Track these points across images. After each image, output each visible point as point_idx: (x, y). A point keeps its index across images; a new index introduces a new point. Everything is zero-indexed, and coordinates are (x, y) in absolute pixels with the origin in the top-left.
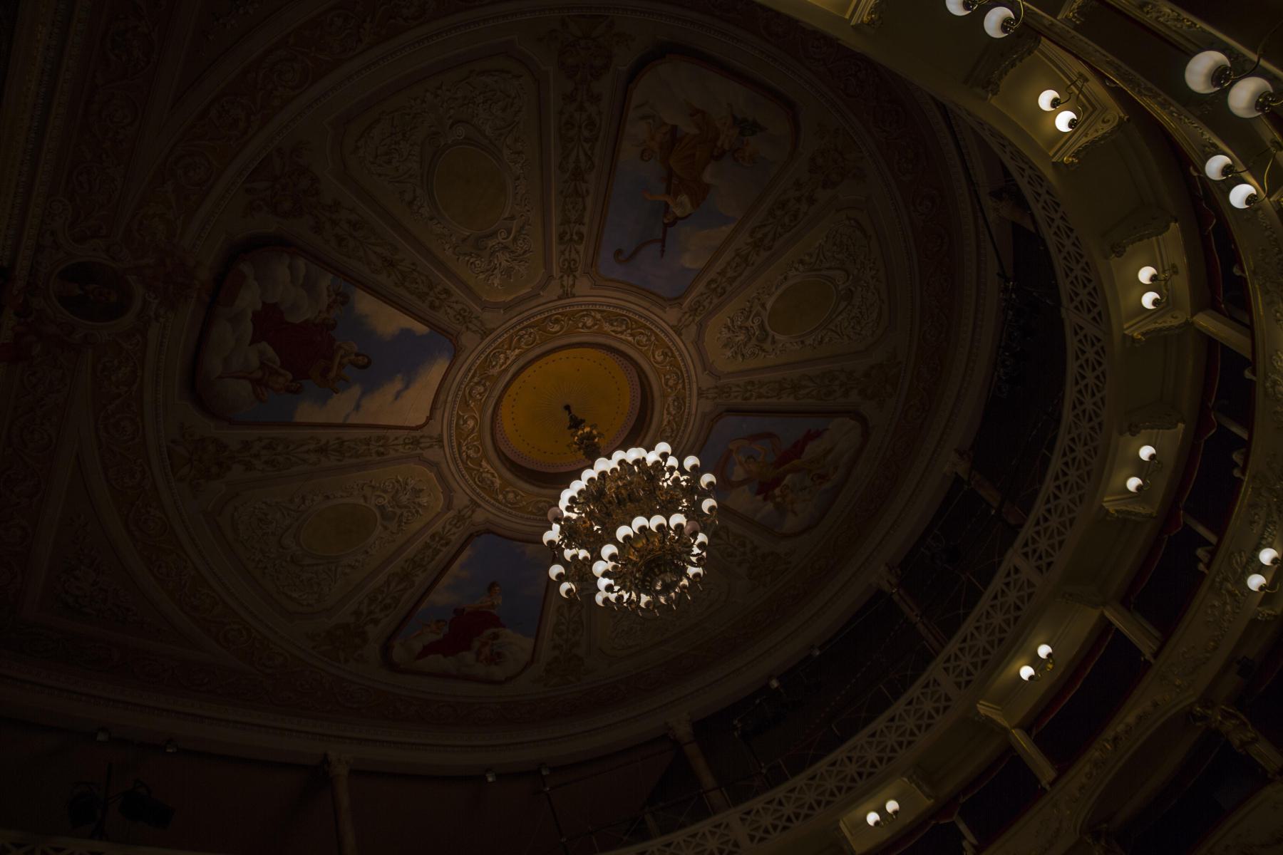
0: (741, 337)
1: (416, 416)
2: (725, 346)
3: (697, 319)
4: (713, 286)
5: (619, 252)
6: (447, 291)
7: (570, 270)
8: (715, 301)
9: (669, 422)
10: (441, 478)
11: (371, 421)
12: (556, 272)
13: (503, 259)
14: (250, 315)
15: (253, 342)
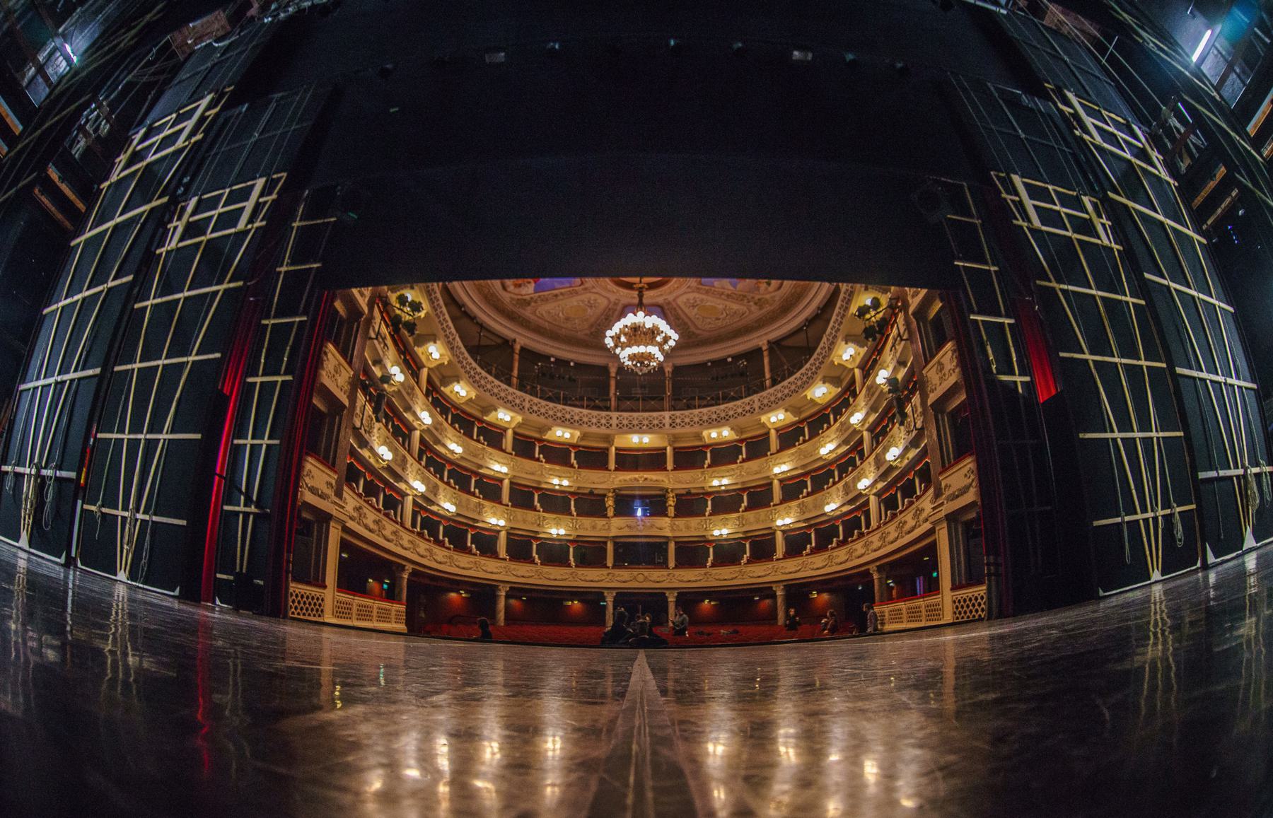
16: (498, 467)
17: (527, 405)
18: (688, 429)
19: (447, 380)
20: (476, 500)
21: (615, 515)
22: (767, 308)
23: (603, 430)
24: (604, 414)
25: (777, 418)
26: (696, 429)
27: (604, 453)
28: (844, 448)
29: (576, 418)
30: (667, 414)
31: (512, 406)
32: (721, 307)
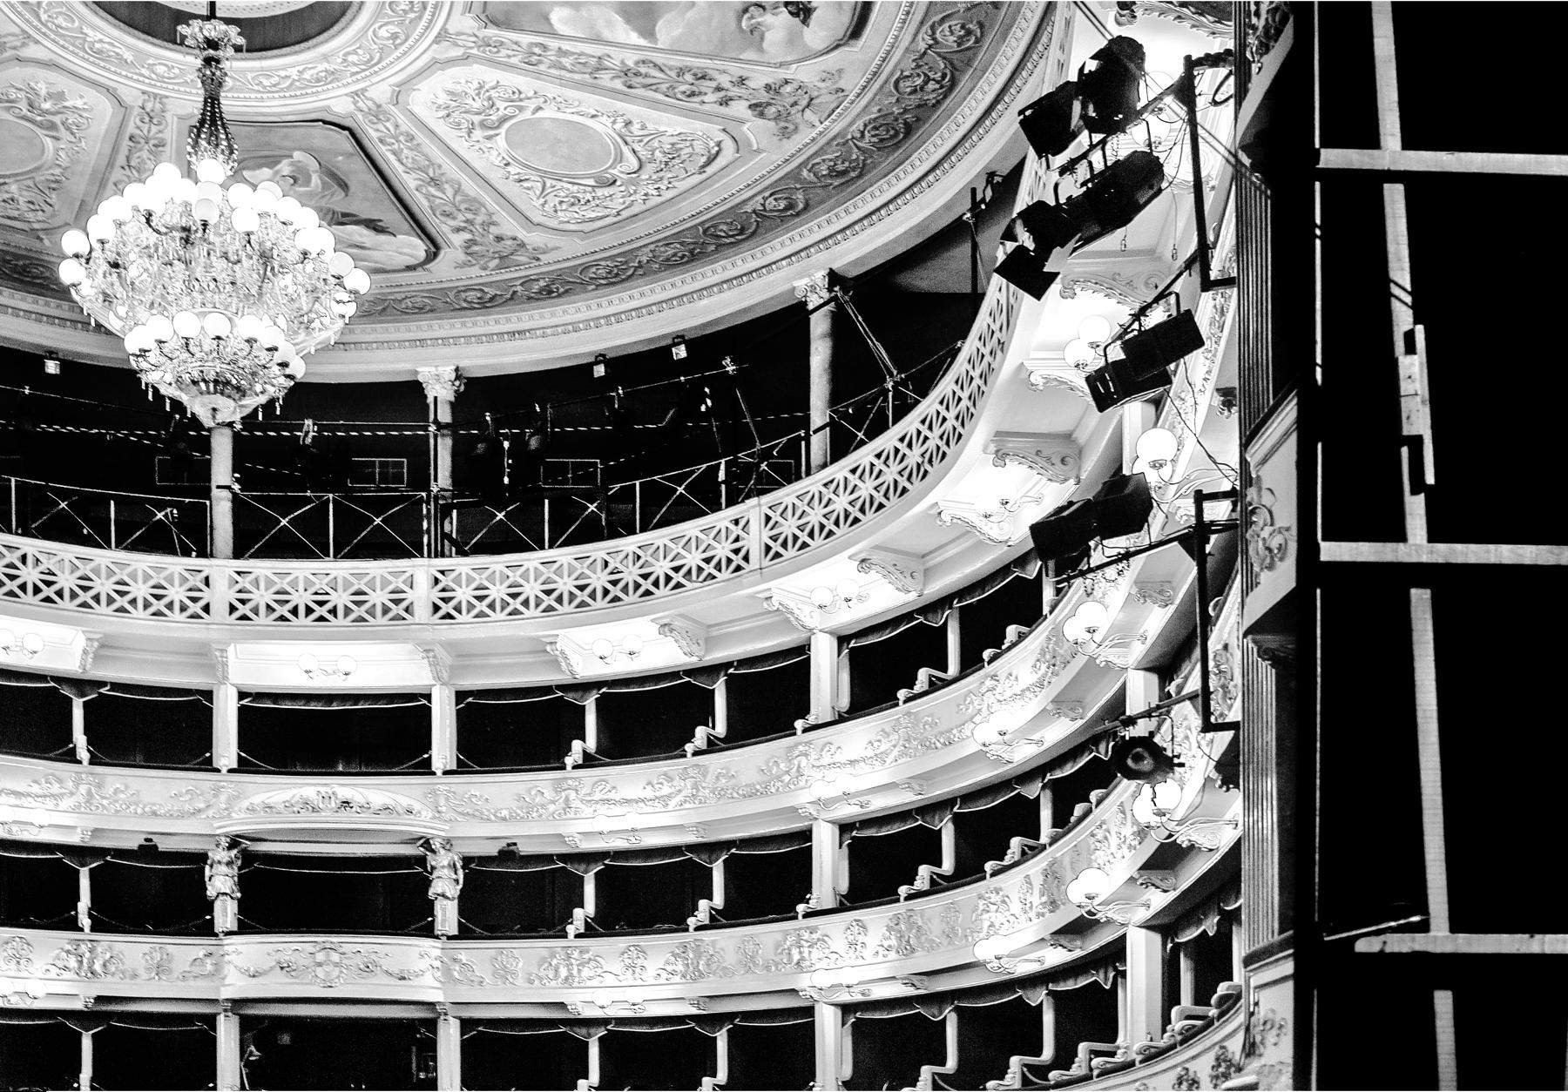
0: (477, 105)
2: (450, 93)
3: (475, 51)
4: (537, 50)
8: (514, 60)
9: (287, 77)
21: (244, 928)
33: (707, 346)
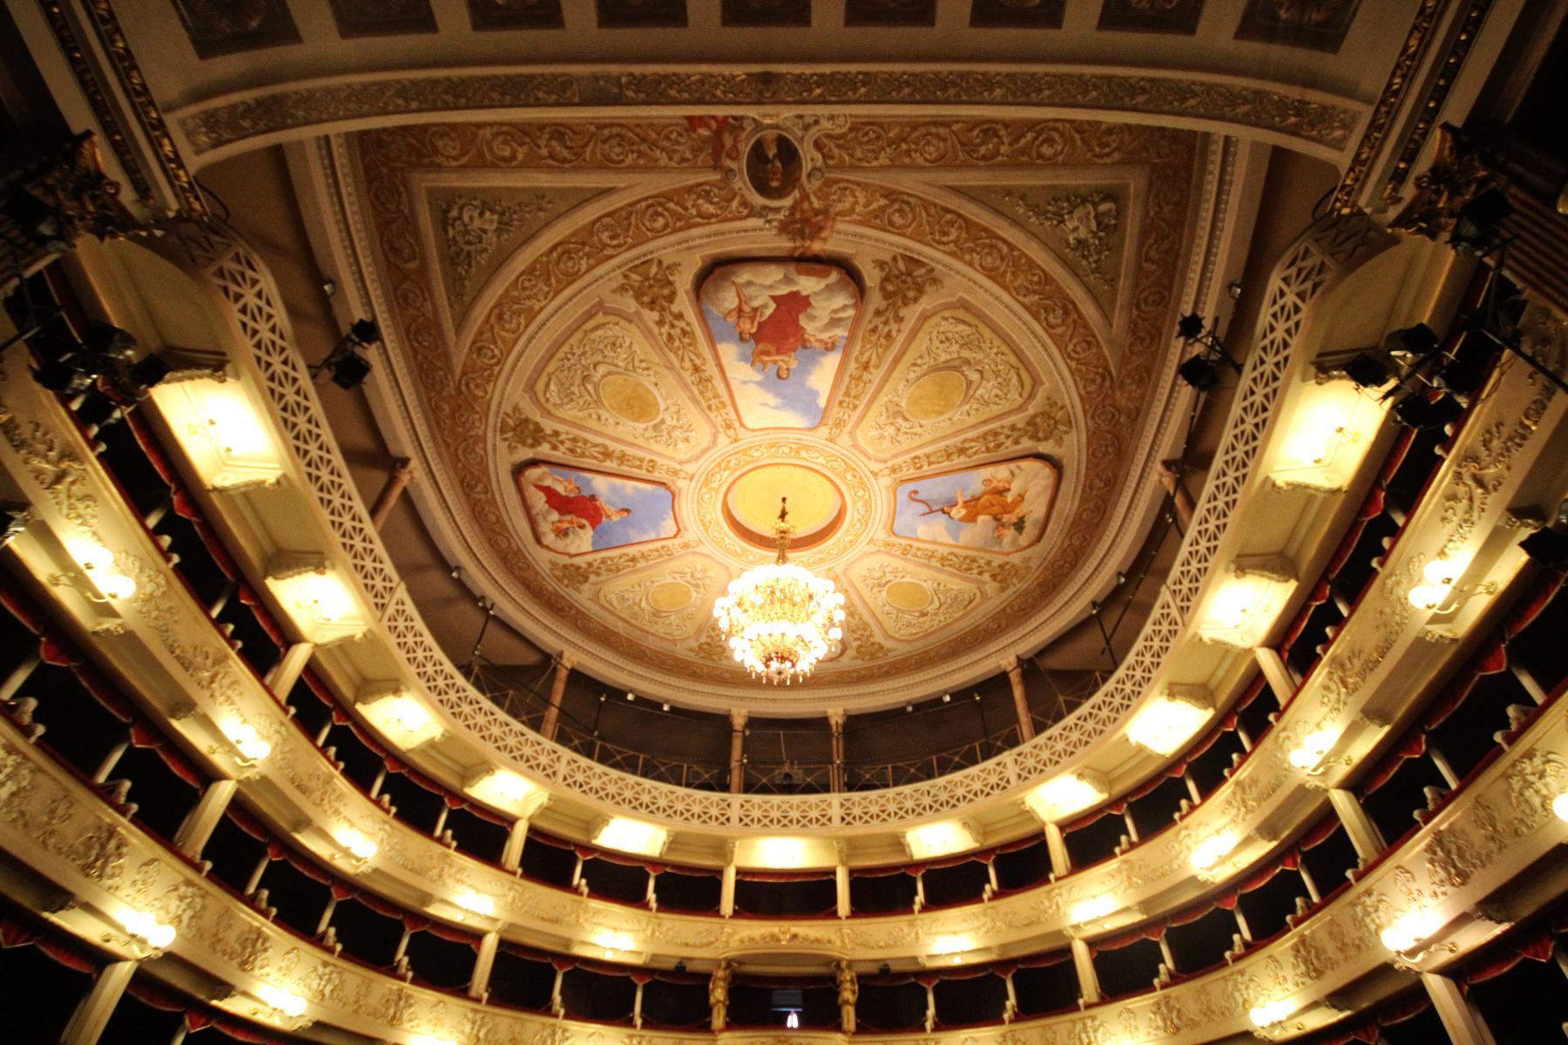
0: (877, 575)
1: (750, 421)
5: (916, 492)
6: (855, 407)
7: (893, 470)
10: (704, 452)
11: (736, 394)
12: (890, 464)
13: (891, 430)
14: (794, 289)
15: (774, 298)
16: (475, 898)
17: (562, 769)
18: (876, 828)
19: (371, 688)
20: (395, 984)
21: (729, 1026)
22: (1016, 586)
23: (713, 829)
24: (716, 796)
25: (1061, 797)
26: (892, 826)
27: (713, 880)
28: (1264, 848)
29: (662, 803)
30: (834, 801)
31: (530, 766)
32: (928, 586)
33: (961, 694)
